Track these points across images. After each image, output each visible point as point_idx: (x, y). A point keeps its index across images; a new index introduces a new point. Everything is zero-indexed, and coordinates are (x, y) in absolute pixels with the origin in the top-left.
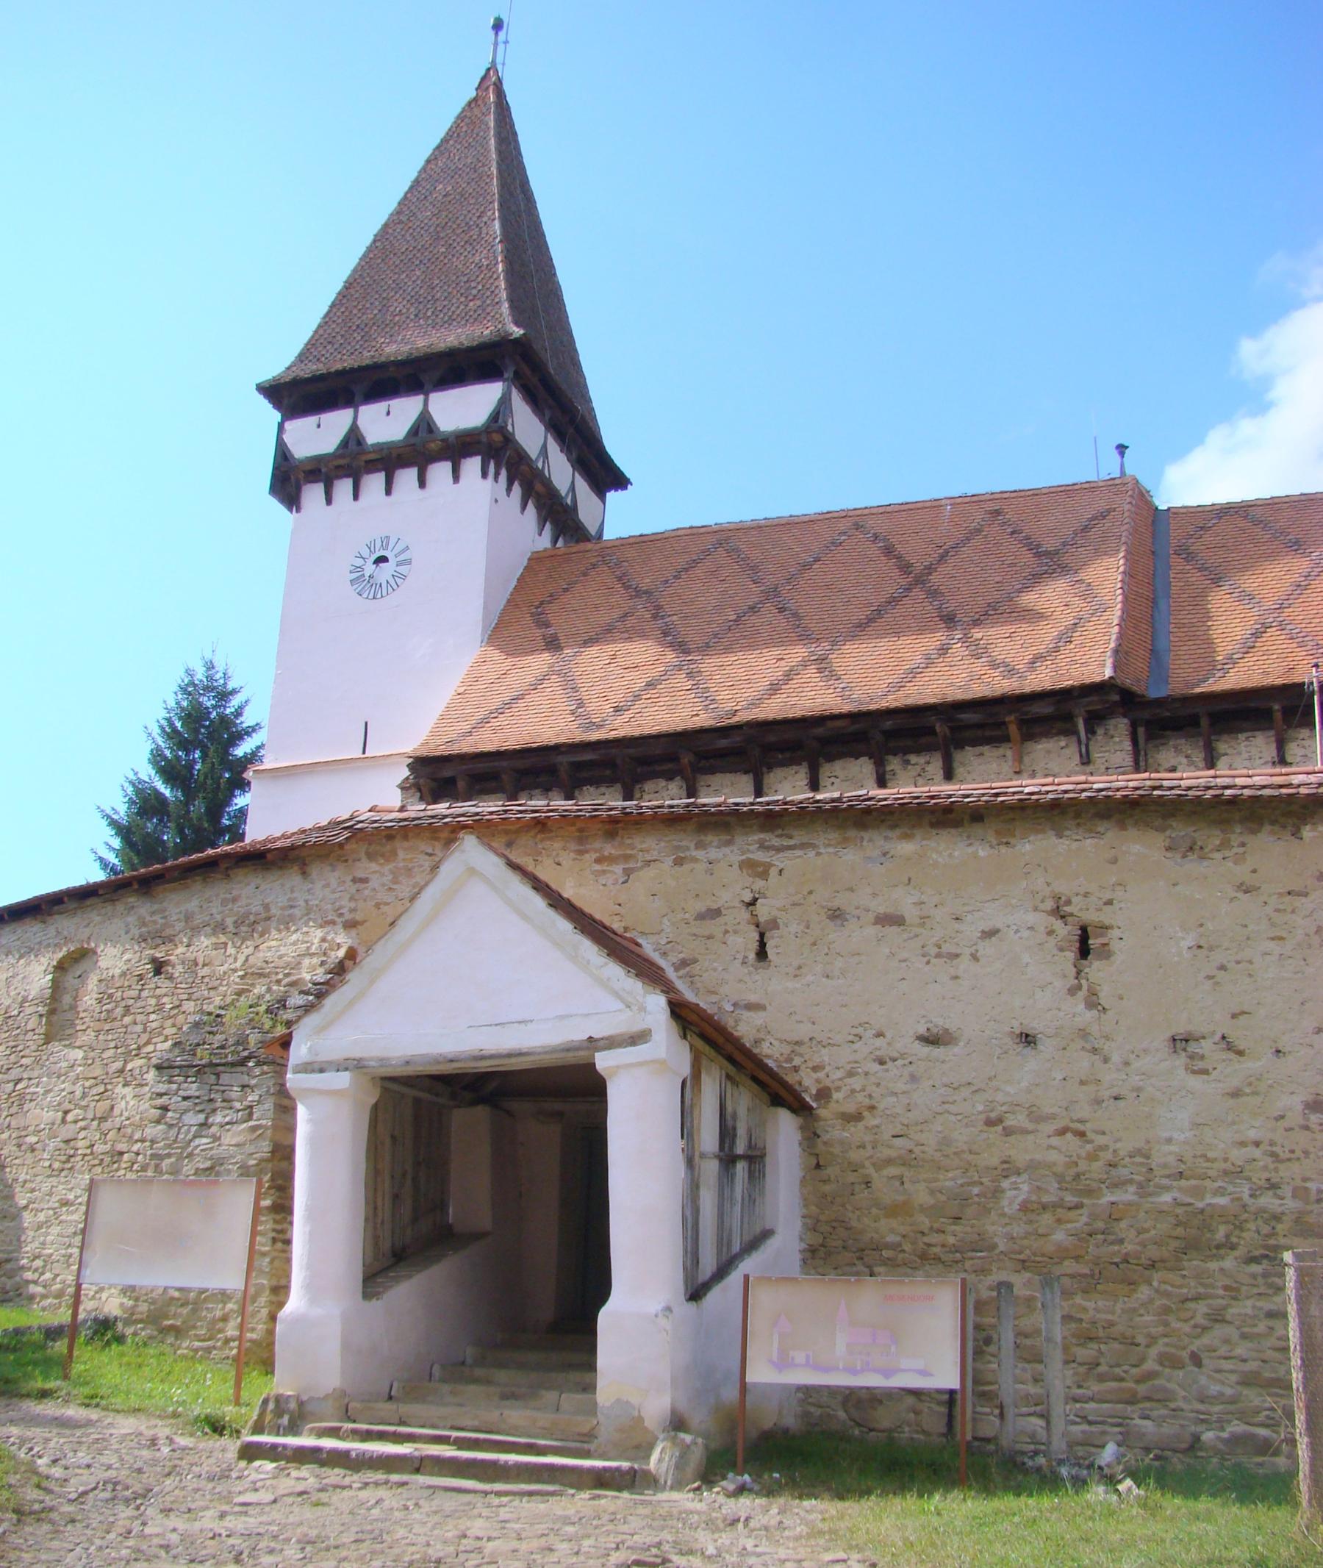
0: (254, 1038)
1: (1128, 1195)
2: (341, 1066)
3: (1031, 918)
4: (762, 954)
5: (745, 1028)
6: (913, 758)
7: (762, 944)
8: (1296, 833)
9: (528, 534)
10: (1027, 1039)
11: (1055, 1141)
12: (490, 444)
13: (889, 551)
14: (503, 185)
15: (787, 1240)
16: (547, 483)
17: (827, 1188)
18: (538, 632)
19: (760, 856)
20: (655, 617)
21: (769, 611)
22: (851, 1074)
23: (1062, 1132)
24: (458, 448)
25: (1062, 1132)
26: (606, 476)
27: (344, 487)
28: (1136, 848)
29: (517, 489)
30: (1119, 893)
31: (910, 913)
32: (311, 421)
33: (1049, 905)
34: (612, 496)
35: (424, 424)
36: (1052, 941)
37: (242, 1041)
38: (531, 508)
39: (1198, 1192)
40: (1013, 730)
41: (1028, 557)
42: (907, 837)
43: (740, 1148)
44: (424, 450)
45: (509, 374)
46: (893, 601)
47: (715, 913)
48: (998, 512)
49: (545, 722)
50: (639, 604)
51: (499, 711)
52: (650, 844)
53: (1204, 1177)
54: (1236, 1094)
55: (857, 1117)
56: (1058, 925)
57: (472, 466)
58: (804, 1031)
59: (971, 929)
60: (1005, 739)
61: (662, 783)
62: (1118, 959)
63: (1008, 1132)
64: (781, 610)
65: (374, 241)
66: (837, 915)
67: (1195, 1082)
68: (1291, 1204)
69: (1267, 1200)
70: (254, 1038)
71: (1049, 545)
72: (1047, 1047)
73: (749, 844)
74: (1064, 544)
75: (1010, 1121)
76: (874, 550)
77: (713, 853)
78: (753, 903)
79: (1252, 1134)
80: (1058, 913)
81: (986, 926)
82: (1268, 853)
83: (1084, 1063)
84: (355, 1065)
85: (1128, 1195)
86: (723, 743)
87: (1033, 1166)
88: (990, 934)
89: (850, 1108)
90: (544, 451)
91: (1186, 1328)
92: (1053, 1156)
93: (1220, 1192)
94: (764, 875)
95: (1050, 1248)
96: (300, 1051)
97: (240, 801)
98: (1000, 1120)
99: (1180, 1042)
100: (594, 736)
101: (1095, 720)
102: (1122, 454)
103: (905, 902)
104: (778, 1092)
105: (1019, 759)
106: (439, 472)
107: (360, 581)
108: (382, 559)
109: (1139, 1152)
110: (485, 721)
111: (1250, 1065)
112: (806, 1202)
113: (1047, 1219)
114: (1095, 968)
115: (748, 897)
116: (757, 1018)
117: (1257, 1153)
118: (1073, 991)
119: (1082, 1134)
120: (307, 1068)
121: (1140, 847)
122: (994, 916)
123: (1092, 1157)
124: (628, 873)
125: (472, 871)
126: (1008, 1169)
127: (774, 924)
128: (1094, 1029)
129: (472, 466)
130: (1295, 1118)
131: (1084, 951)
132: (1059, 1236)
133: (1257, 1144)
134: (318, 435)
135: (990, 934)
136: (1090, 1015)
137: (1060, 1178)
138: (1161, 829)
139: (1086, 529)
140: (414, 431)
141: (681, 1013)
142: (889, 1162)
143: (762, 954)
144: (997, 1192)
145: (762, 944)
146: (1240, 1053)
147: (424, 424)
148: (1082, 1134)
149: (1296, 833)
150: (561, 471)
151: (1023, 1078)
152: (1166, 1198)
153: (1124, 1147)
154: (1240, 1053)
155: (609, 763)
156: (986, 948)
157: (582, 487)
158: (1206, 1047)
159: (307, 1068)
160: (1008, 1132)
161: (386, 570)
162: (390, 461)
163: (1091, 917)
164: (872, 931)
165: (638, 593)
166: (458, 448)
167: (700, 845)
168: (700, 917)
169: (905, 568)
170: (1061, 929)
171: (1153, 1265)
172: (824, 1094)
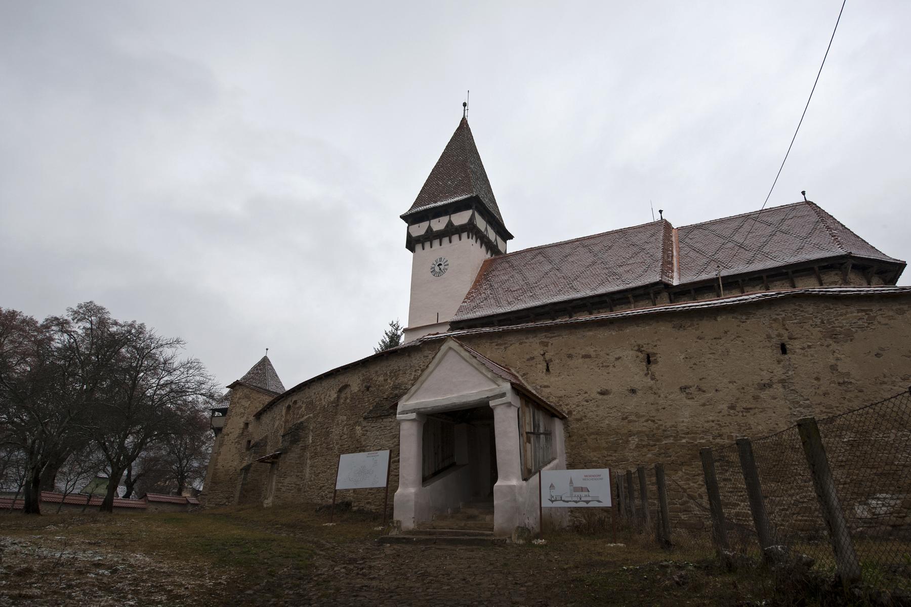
1: (671, 440)
3: (631, 352)
4: (548, 370)
5: (543, 395)
7: (548, 367)
8: (716, 319)
10: (633, 391)
11: (645, 424)
12: (470, 229)
15: (561, 458)
16: (488, 238)
17: (573, 443)
19: (545, 340)
22: (578, 406)
23: (647, 421)
25: (647, 421)
26: (507, 236)
27: (427, 245)
28: (663, 328)
29: (479, 241)
30: (659, 343)
31: (593, 354)
32: (417, 225)
33: (636, 348)
34: (508, 241)
35: (450, 223)
36: (638, 359)
38: (483, 246)
39: (694, 439)
40: (632, 300)
42: (589, 330)
43: (542, 430)
44: (451, 231)
47: (533, 358)
52: (512, 339)
53: (696, 433)
54: (704, 405)
55: (581, 420)
56: (640, 354)
57: (465, 235)
58: (562, 393)
59: (612, 358)
60: (629, 303)
63: (630, 422)
66: (570, 356)
67: (689, 402)
68: (727, 441)
69: (718, 440)
72: (640, 393)
73: (542, 337)
75: (630, 418)
77: (531, 340)
78: (543, 355)
79: (711, 418)
80: (639, 350)
81: (617, 356)
82: (707, 327)
83: (652, 398)
85: (671, 440)
87: (639, 433)
88: (618, 359)
89: (578, 416)
91: (696, 485)
92: (644, 429)
93: (703, 438)
94: (547, 346)
95: (647, 460)
98: (626, 418)
99: (683, 389)
101: (657, 293)
103: (591, 351)
104: (551, 413)
107: (433, 271)
109: (673, 426)
112: (567, 448)
113: (645, 450)
114: (653, 367)
115: (542, 352)
116: (547, 390)
117: (713, 424)
118: (646, 375)
119: (654, 421)
120: (403, 413)
121: (664, 328)
122: (618, 353)
123: (658, 429)
124: (505, 348)
125: (450, 348)
126: (631, 434)
127: (551, 360)
130: (725, 412)
131: (649, 362)
132: (649, 455)
133: (713, 421)
134: (420, 230)
135: (618, 359)
136: (652, 382)
137: (647, 436)
138: (670, 322)
141: (518, 389)
142: (592, 433)
143: (548, 370)
144: (627, 442)
145: (548, 367)
146: (704, 391)
147: (450, 223)
148: (654, 421)
149: (716, 319)
150: (492, 235)
151: (632, 404)
152: (684, 441)
153: (669, 424)
154: (704, 391)
156: (617, 363)
157: (499, 239)
158: (693, 390)
159: (404, 412)
160: (630, 422)
163: (650, 351)
164: (580, 360)
167: (527, 338)
168: (528, 360)
170: (641, 356)
171: (682, 464)
172: (570, 413)
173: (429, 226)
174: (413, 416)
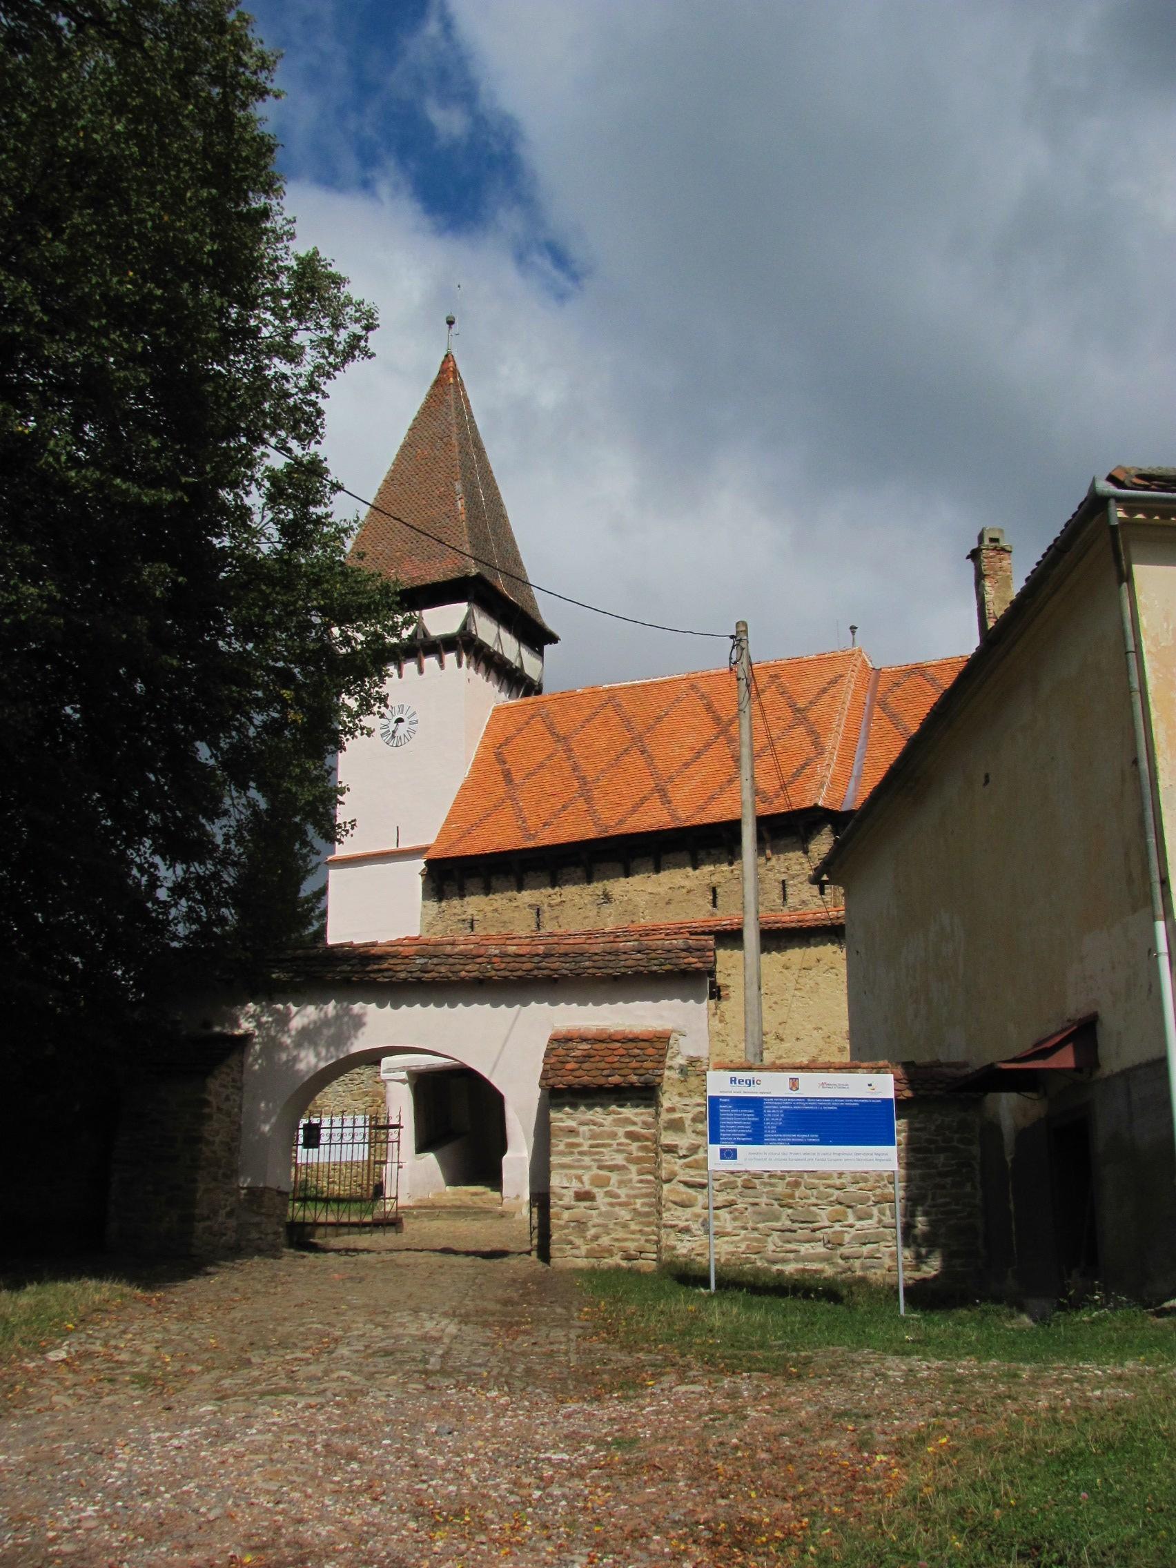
6: (713, 852)
9: (489, 695)
12: (463, 643)
13: (709, 707)
34: (546, 647)
41: (788, 713)
46: (708, 745)
48: (776, 676)
50: (559, 746)
61: (573, 869)
62: (732, 1000)
64: (643, 752)
65: (380, 493)
74: (811, 702)
76: (699, 706)
100: (531, 844)
102: (853, 633)
111: (786, 1045)
114: (724, 1005)
120: (389, 1071)
128: (723, 1032)
136: (720, 1025)
150: (509, 647)
157: (525, 652)
159: (389, 1071)
169: (717, 720)
174: (404, 1075)
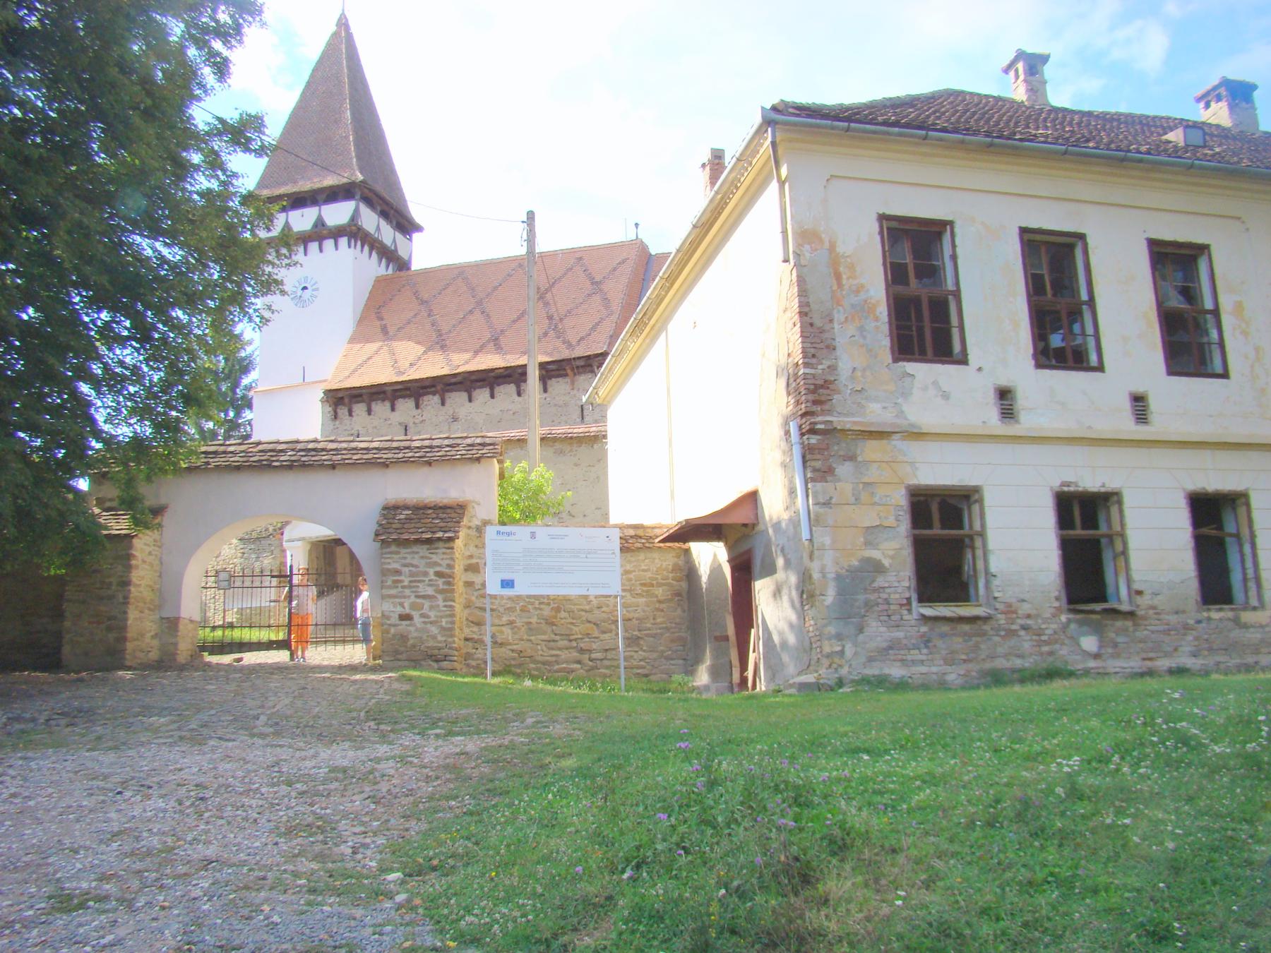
0: (271, 529)
2: (299, 540)
9: (374, 268)
12: (353, 232)
14: (351, 84)
16: (381, 243)
18: (378, 323)
20: (429, 315)
21: (477, 313)
24: (337, 233)
35: (320, 223)
37: (267, 530)
44: (320, 234)
45: (358, 197)
48: (581, 259)
49: (381, 373)
51: (361, 365)
57: (343, 241)
60: (566, 375)
70: (271, 529)
71: (598, 279)
84: (302, 539)
86: (453, 380)
90: (378, 228)
96: (286, 537)
97: (245, 381)
105: (573, 383)
106: (329, 244)
108: (305, 288)
110: (355, 370)
129: (343, 241)
139: (615, 269)
140: (315, 225)
147: (320, 223)
150: (387, 234)
155: (407, 389)
161: (308, 293)
162: (305, 239)
165: (423, 302)
166: (337, 233)
173: (287, 222)
